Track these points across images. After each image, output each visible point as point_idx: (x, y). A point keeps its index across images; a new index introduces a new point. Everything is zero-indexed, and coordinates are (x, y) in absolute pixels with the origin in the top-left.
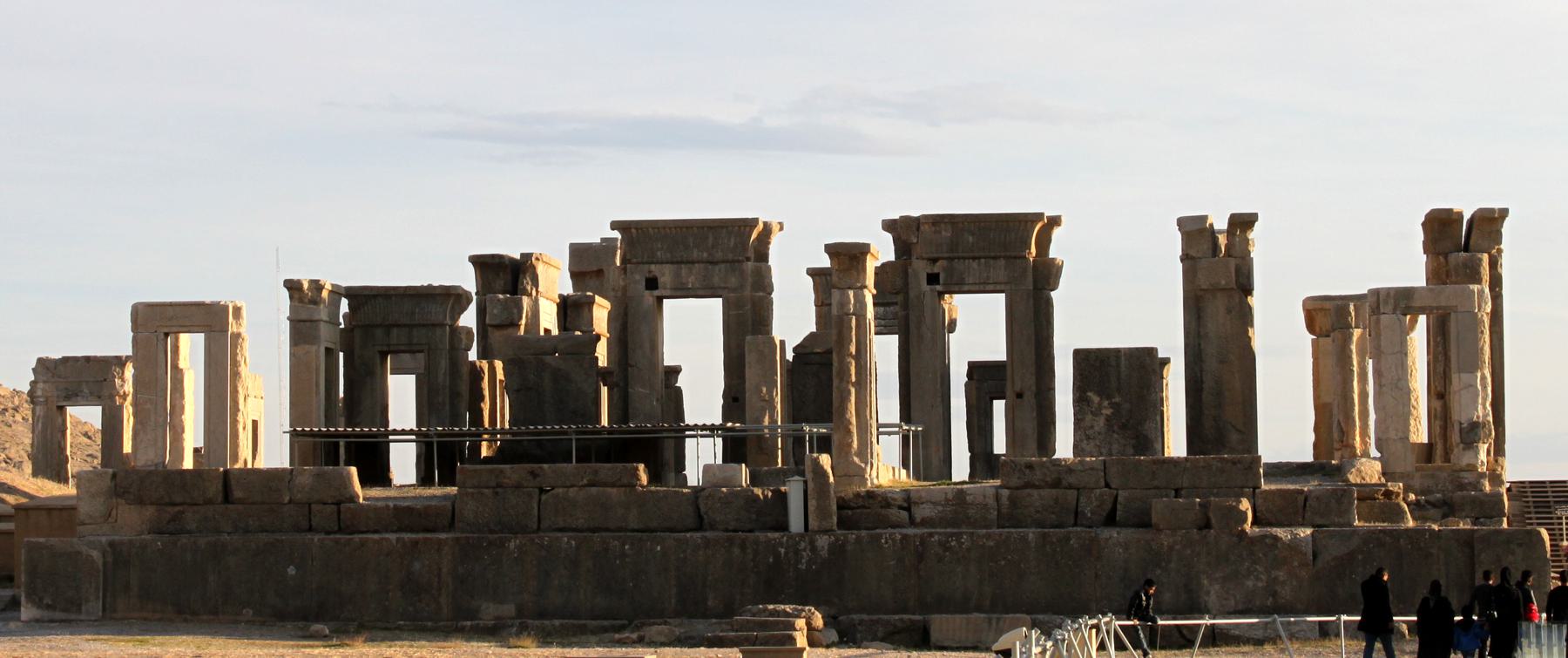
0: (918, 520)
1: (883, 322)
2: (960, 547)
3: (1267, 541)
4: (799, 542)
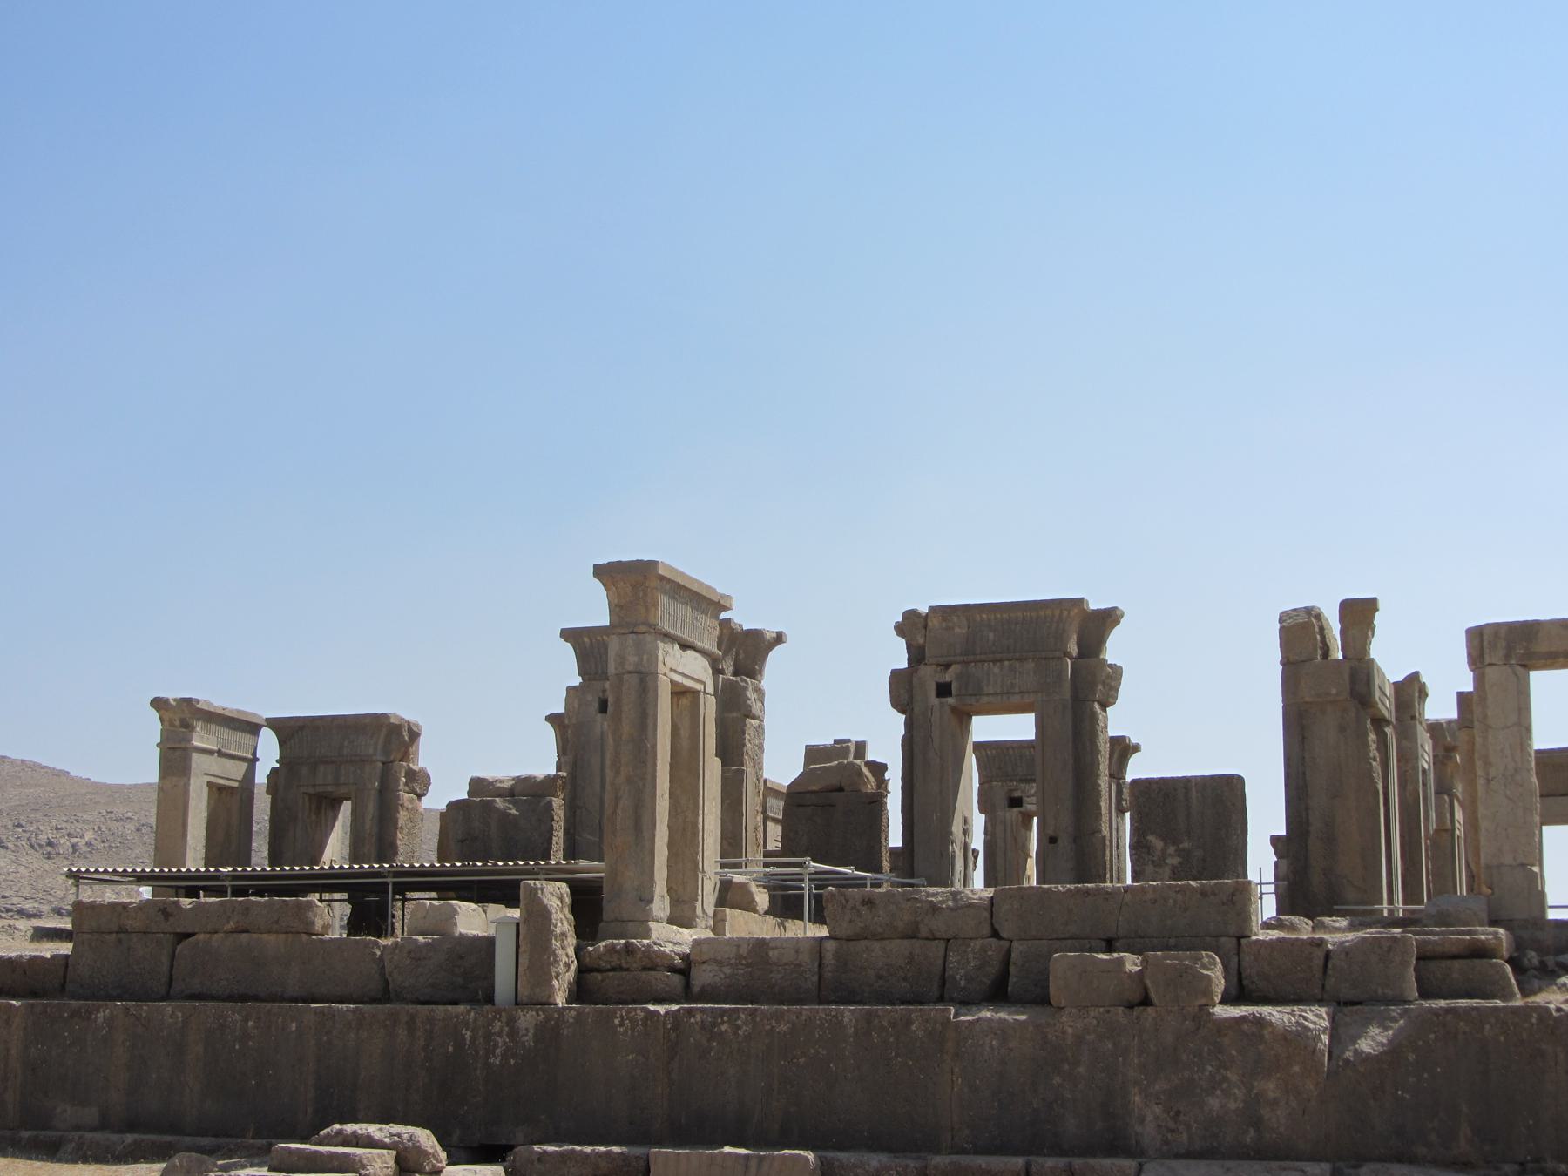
2: (736, 1033)
3: (1245, 1027)
4: (493, 1021)
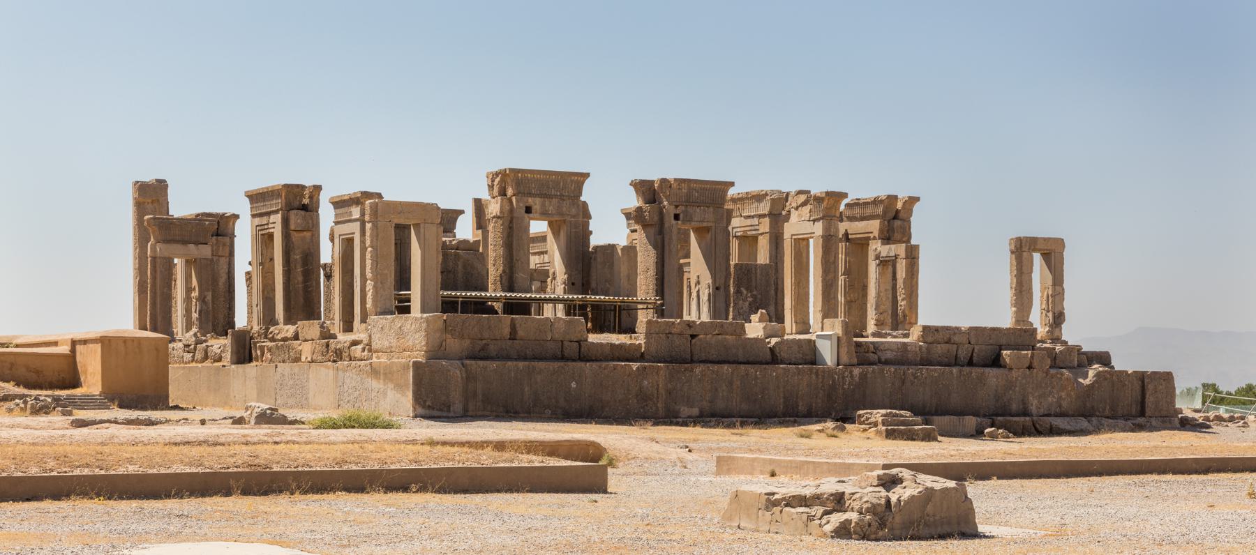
0: (883, 360)
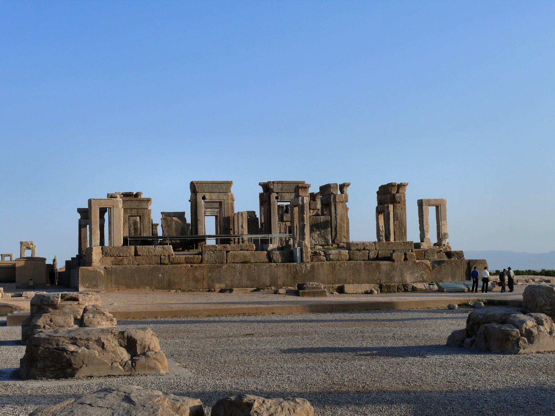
1: (211, 213)
